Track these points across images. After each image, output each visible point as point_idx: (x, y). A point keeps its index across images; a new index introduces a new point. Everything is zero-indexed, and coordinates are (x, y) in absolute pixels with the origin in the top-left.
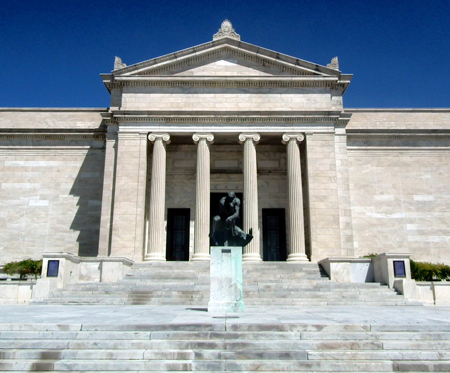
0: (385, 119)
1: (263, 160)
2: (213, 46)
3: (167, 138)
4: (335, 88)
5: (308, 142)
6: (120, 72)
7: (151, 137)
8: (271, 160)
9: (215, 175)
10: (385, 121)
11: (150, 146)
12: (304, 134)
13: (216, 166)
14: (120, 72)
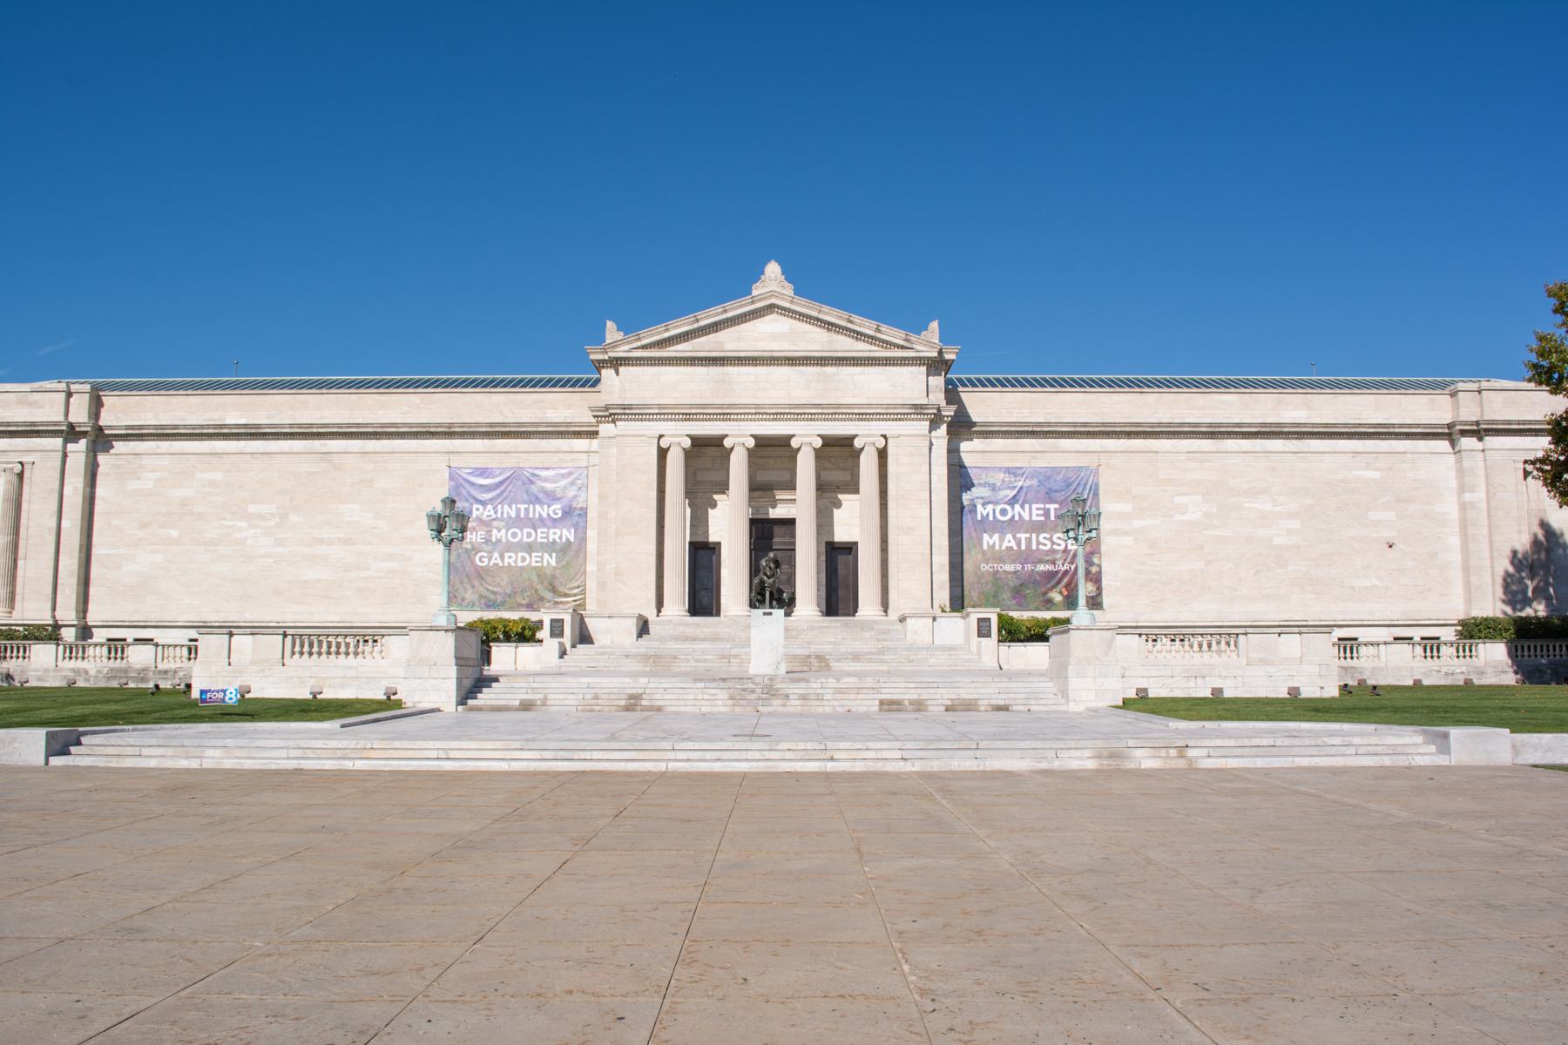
0: (1014, 405)
1: (827, 469)
2: (753, 302)
3: (687, 443)
4: (935, 366)
5: (890, 450)
6: (615, 345)
7: (664, 444)
8: (840, 469)
9: (757, 494)
10: (1014, 408)
11: (662, 454)
12: (884, 436)
13: (758, 479)
14: (615, 345)
